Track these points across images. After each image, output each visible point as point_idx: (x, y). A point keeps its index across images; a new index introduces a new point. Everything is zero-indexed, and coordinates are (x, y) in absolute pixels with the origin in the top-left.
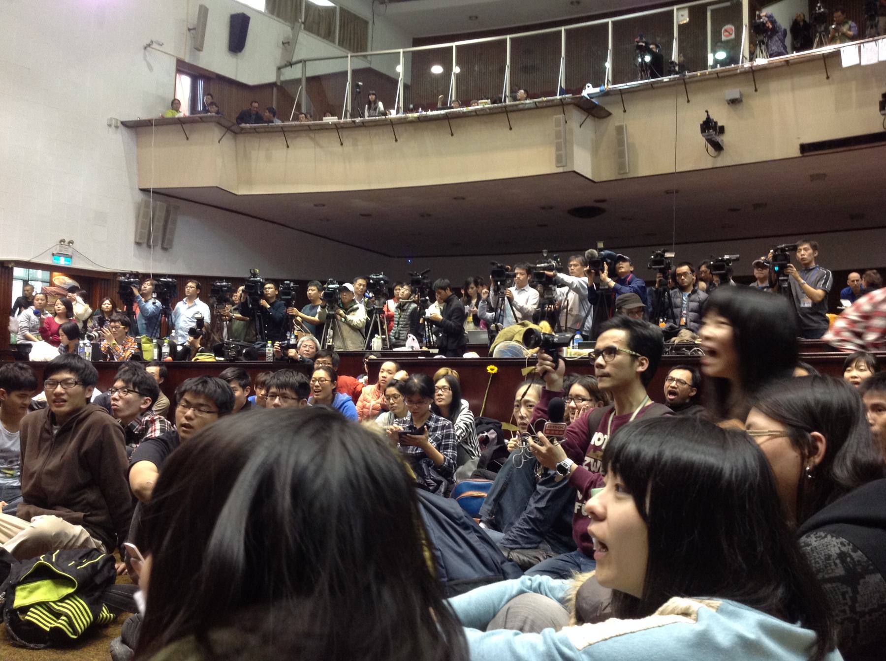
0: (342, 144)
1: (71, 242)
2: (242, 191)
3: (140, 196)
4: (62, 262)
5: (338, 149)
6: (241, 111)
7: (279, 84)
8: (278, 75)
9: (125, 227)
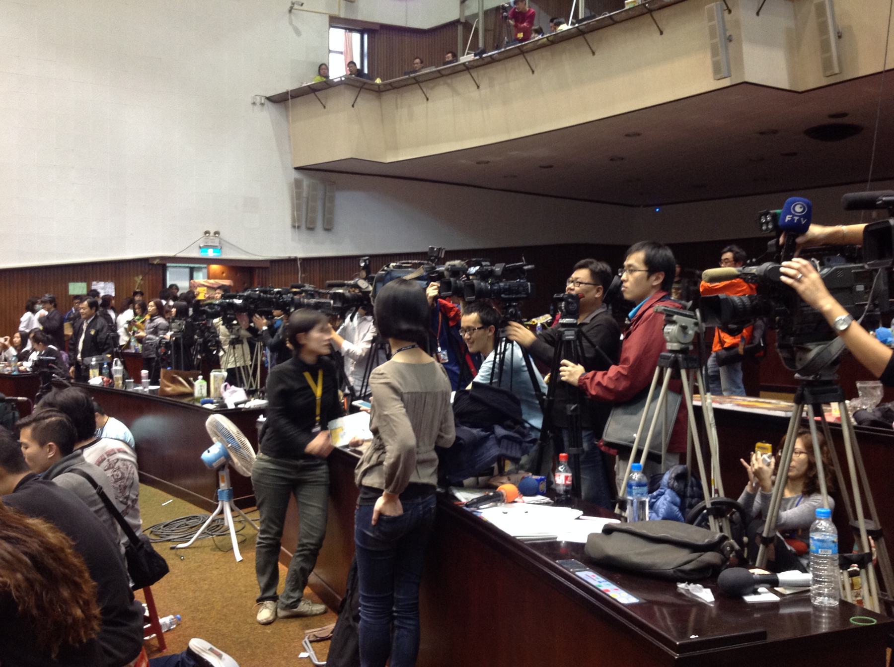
0: (478, 87)
1: (216, 233)
2: (390, 159)
3: (295, 175)
4: (211, 254)
5: (474, 93)
6: (401, 59)
7: (463, 20)
8: (462, 11)
9: (281, 209)
